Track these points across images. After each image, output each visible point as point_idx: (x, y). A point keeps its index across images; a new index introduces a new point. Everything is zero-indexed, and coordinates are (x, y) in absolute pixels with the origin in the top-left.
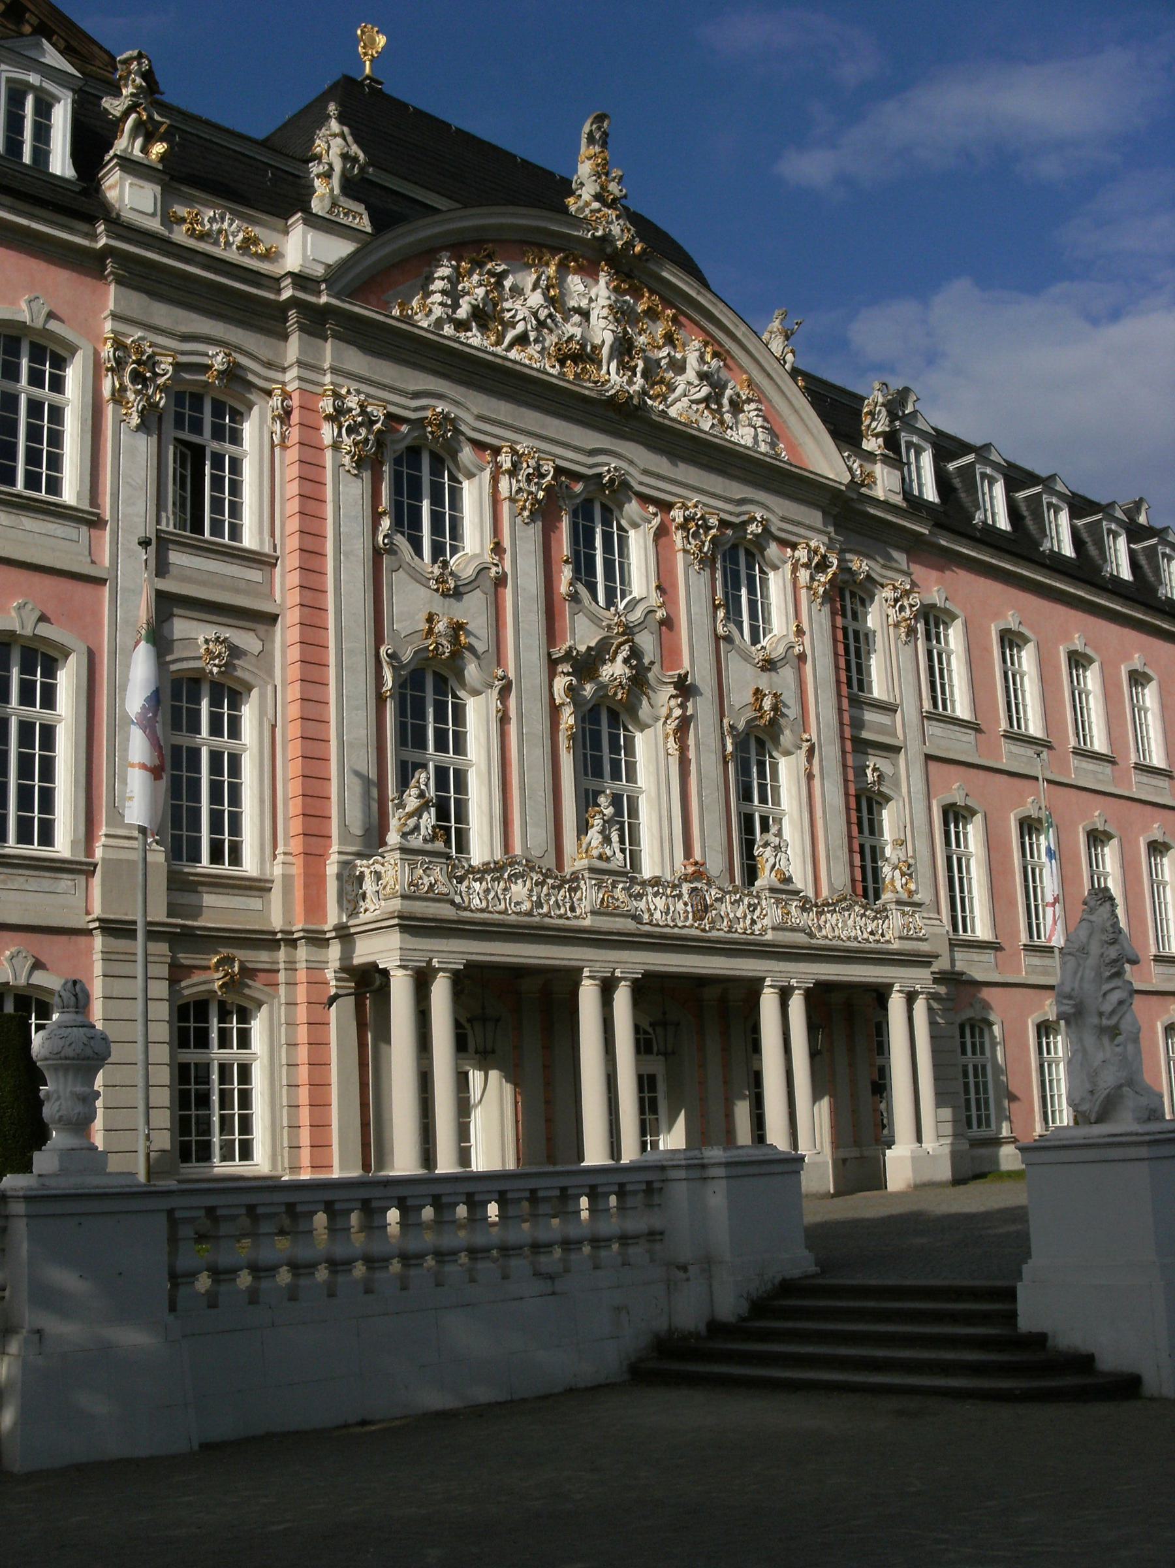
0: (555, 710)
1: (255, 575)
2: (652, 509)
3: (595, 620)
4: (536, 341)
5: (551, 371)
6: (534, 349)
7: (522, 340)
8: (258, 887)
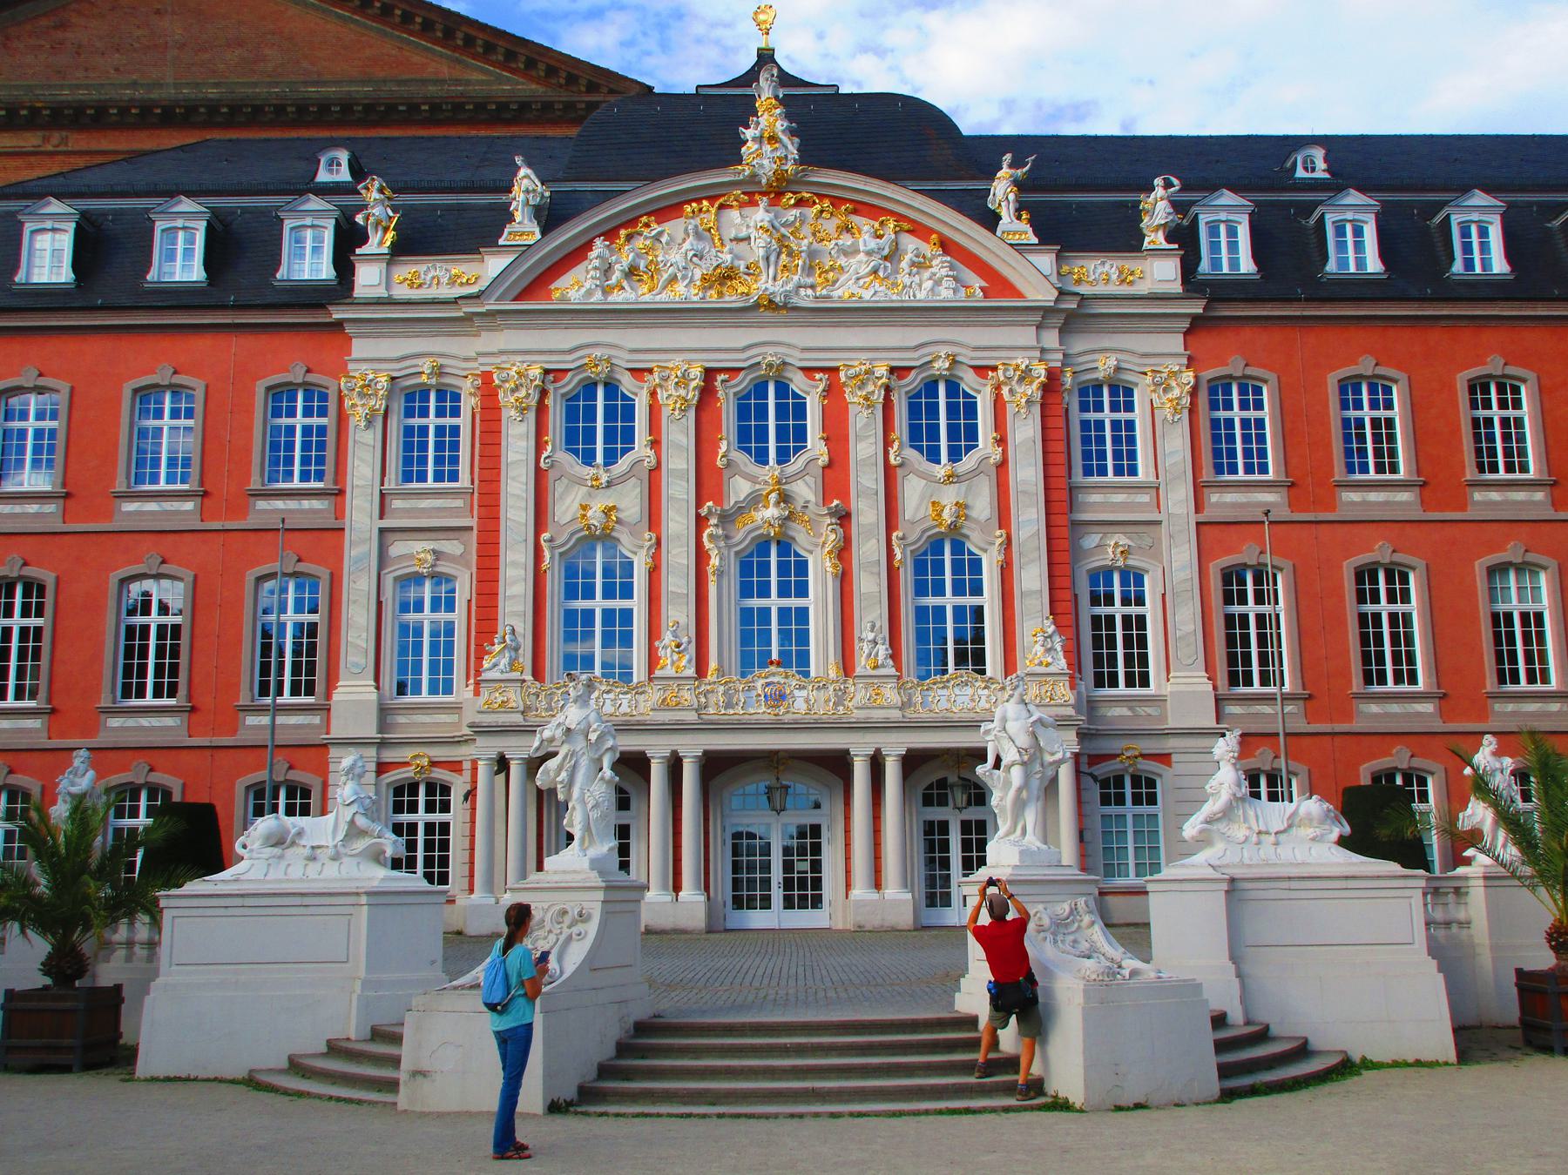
0: (701, 556)
1: (459, 503)
2: (818, 376)
3: (753, 479)
4: (684, 277)
5: (695, 299)
6: (680, 287)
7: (673, 279)
8: (456, 708)
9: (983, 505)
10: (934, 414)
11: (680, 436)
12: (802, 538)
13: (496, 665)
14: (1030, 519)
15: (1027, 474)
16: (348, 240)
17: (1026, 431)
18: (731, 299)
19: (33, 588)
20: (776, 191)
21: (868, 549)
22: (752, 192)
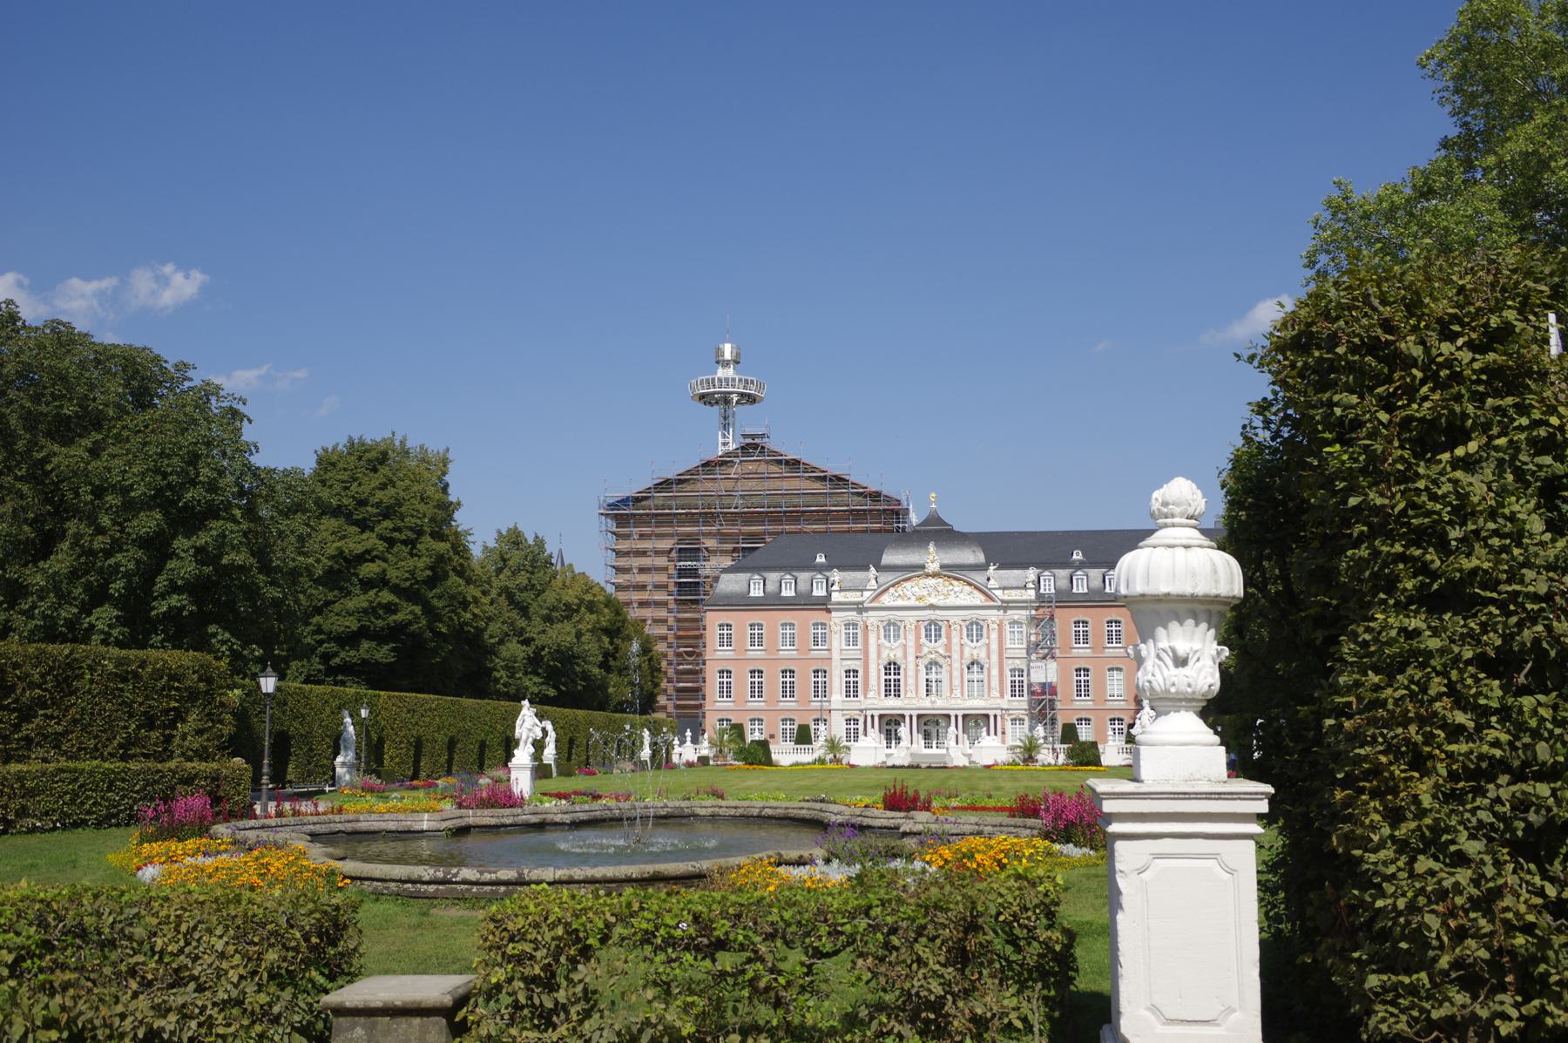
9: (983, 654)
10: (975, 629)
11: (911, 637)
12: (941, 661)
13: (871, 694)
14: (995, 657)
15: (994, 647)
16: (830, 584)
17: (994, 635)
18: (921, 604)
19: (760, 672)
20: (935, 575)
21: (956, 665)
22: (928, 575)
